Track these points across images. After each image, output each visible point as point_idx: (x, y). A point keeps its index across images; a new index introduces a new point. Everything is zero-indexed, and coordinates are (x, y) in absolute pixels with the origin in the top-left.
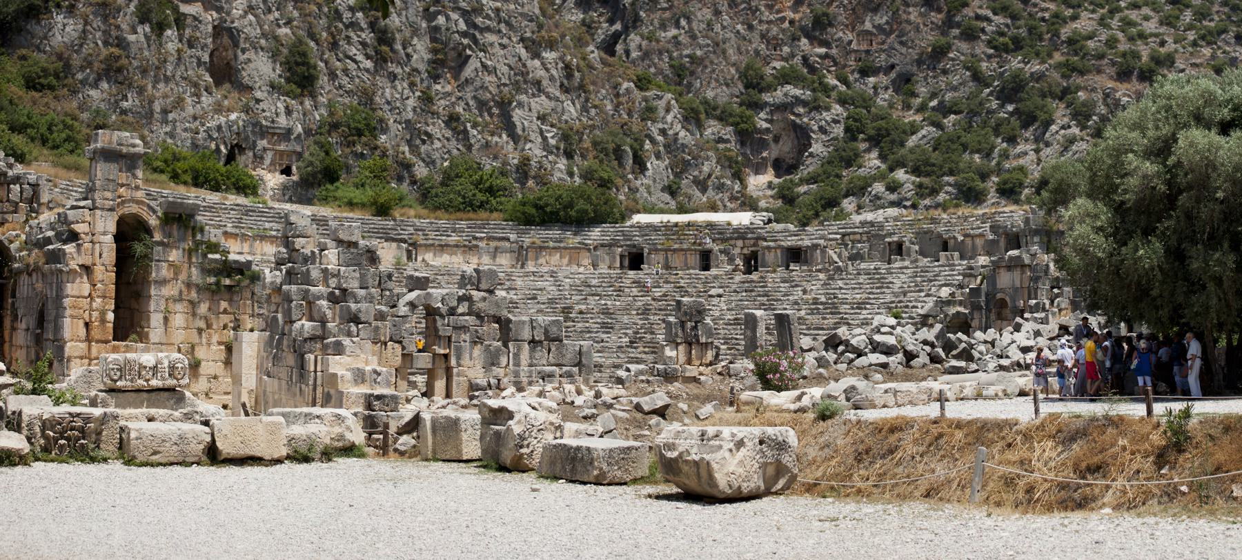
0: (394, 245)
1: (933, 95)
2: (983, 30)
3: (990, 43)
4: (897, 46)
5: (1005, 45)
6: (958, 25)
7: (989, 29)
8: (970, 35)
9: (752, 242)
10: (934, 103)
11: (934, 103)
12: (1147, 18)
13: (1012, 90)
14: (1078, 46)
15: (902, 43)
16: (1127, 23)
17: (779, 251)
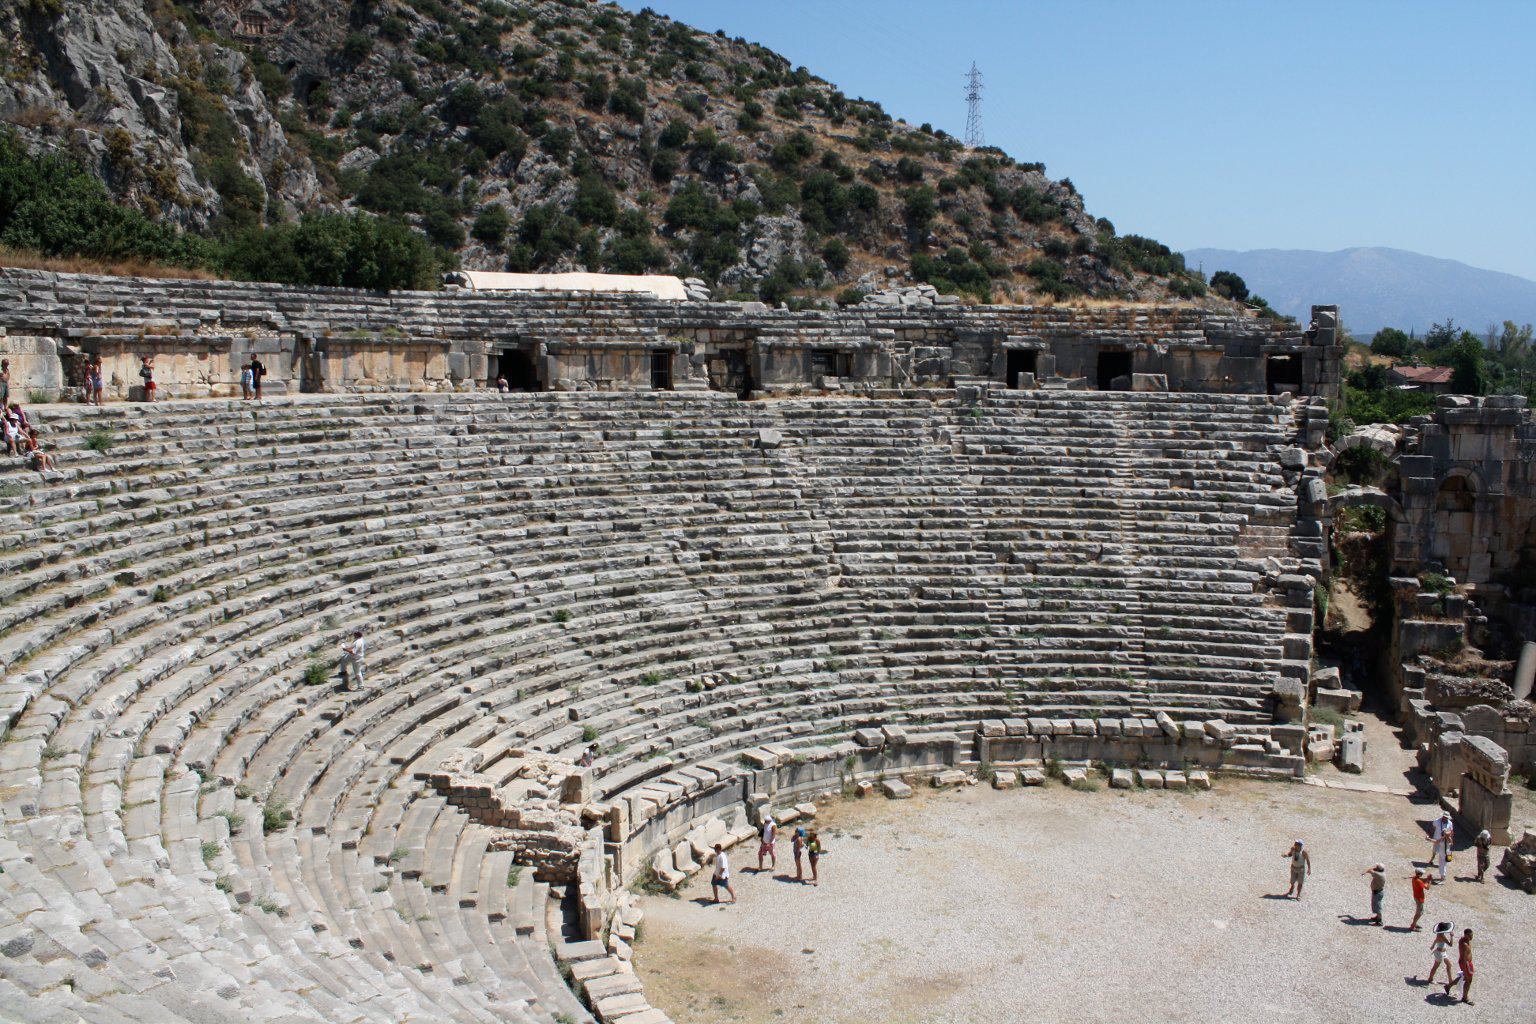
0: (31, 341)
1: (354, 107)
2: (408, 30)
3: (420, 48)
4: (297, 36)
5: (439, 53)
6: (377, 21)
7: (415, 30)
8: (393, 33)
9: (725, 334)
10: (357, 117)
11: (357, 117)
12: (585, 40)
13: (460, 108)
14: (527, 63)
15: (304, 34)
16: (569, 44)
17: (798, 355)
